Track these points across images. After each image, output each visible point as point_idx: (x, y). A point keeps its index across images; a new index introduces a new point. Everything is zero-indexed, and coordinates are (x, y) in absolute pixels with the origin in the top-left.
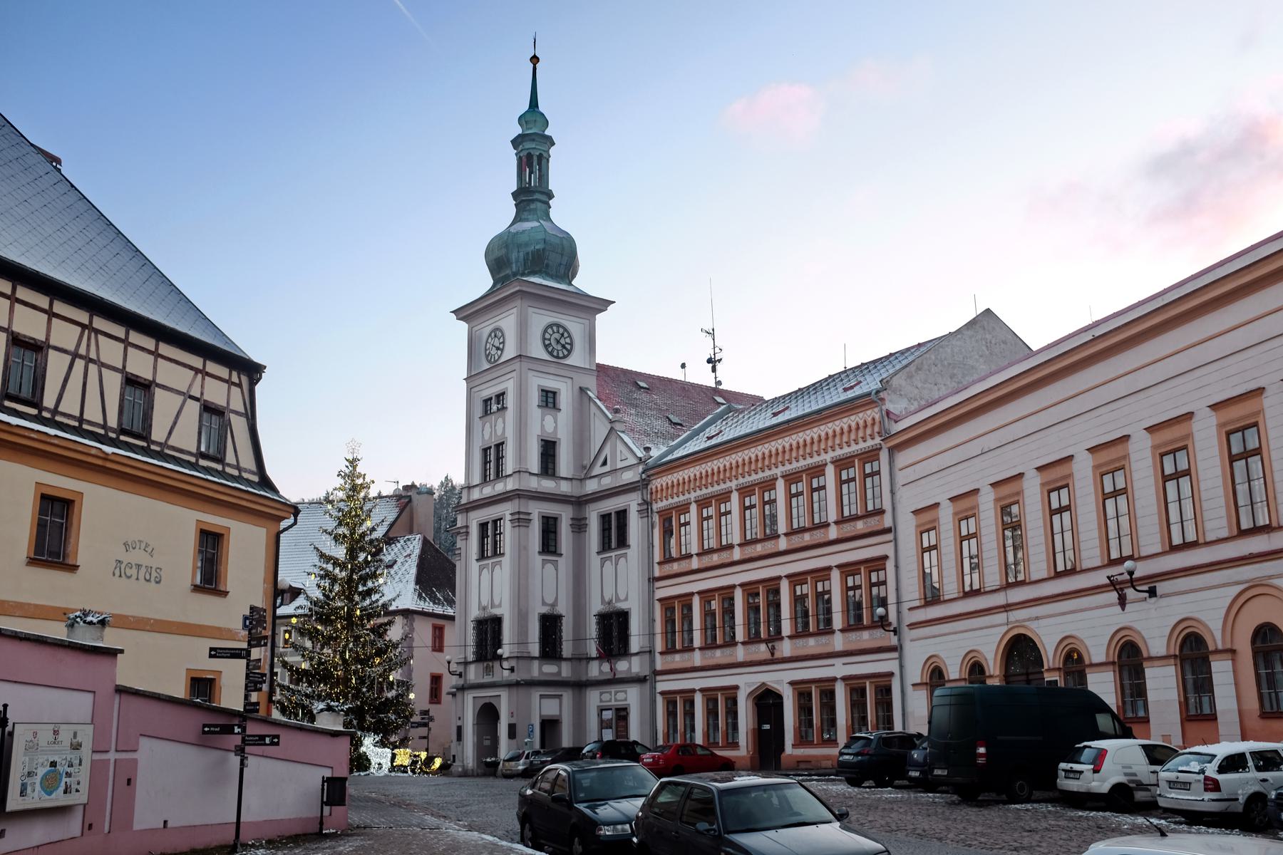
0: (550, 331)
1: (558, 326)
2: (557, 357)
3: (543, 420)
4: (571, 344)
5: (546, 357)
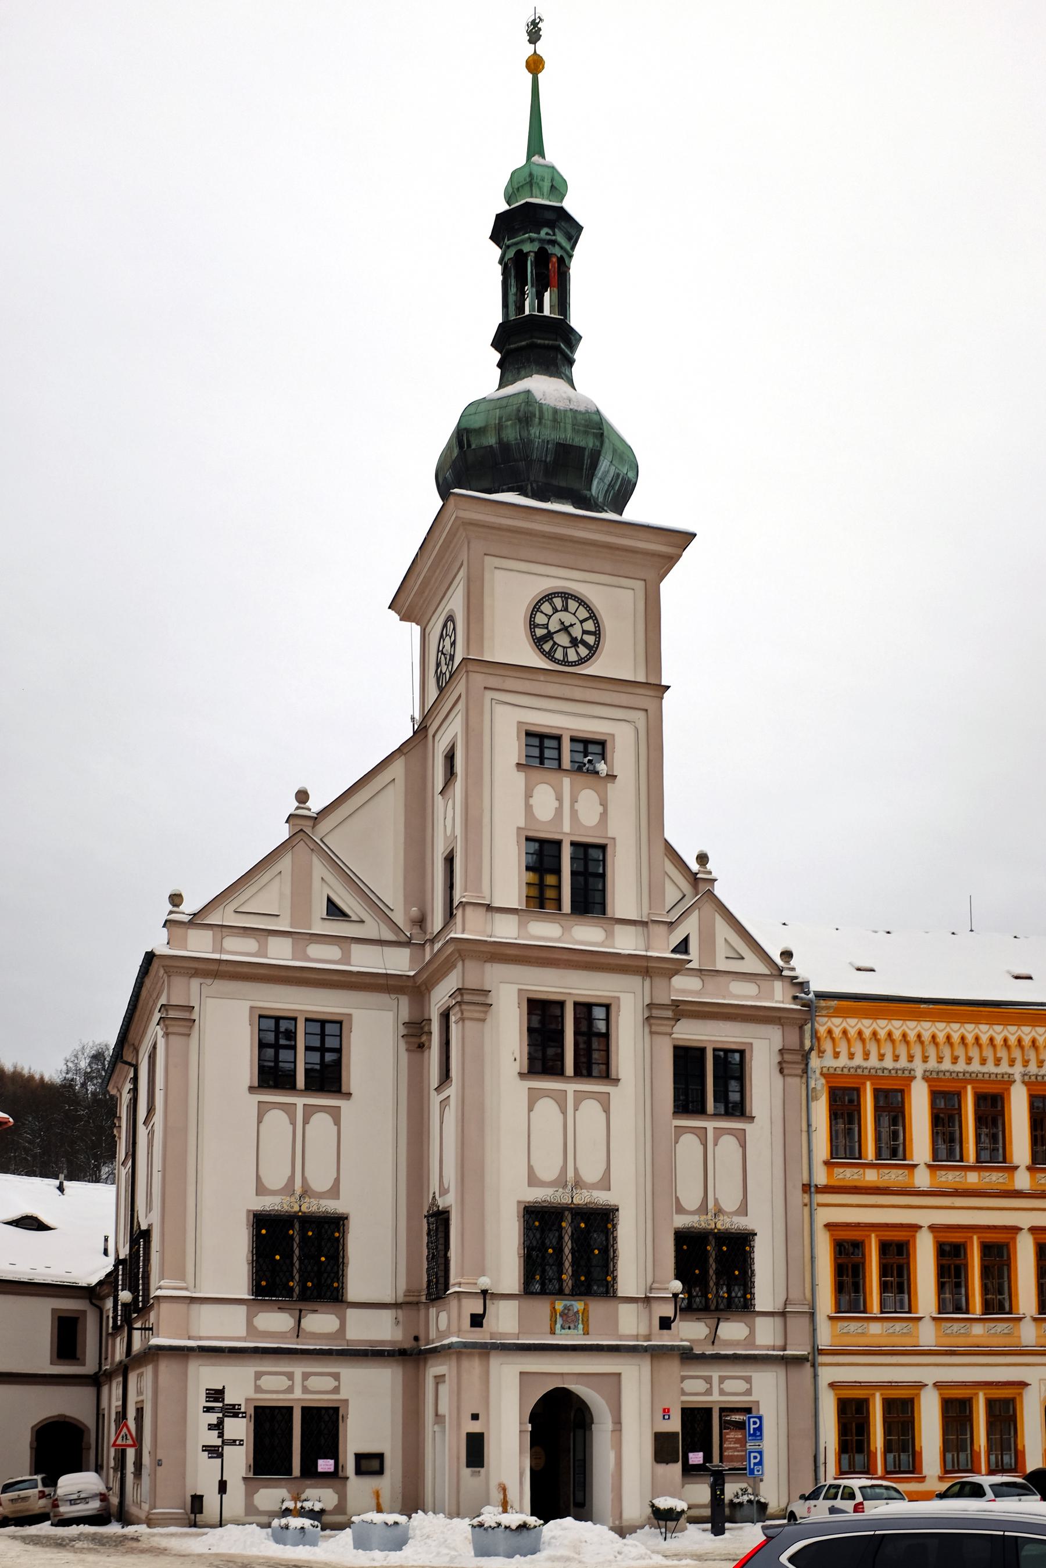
0: (546, 608)
1: (566, 596)
2: (565, 662)
3: (528, 795)
4: (597, 633)
5: (539, 662)
